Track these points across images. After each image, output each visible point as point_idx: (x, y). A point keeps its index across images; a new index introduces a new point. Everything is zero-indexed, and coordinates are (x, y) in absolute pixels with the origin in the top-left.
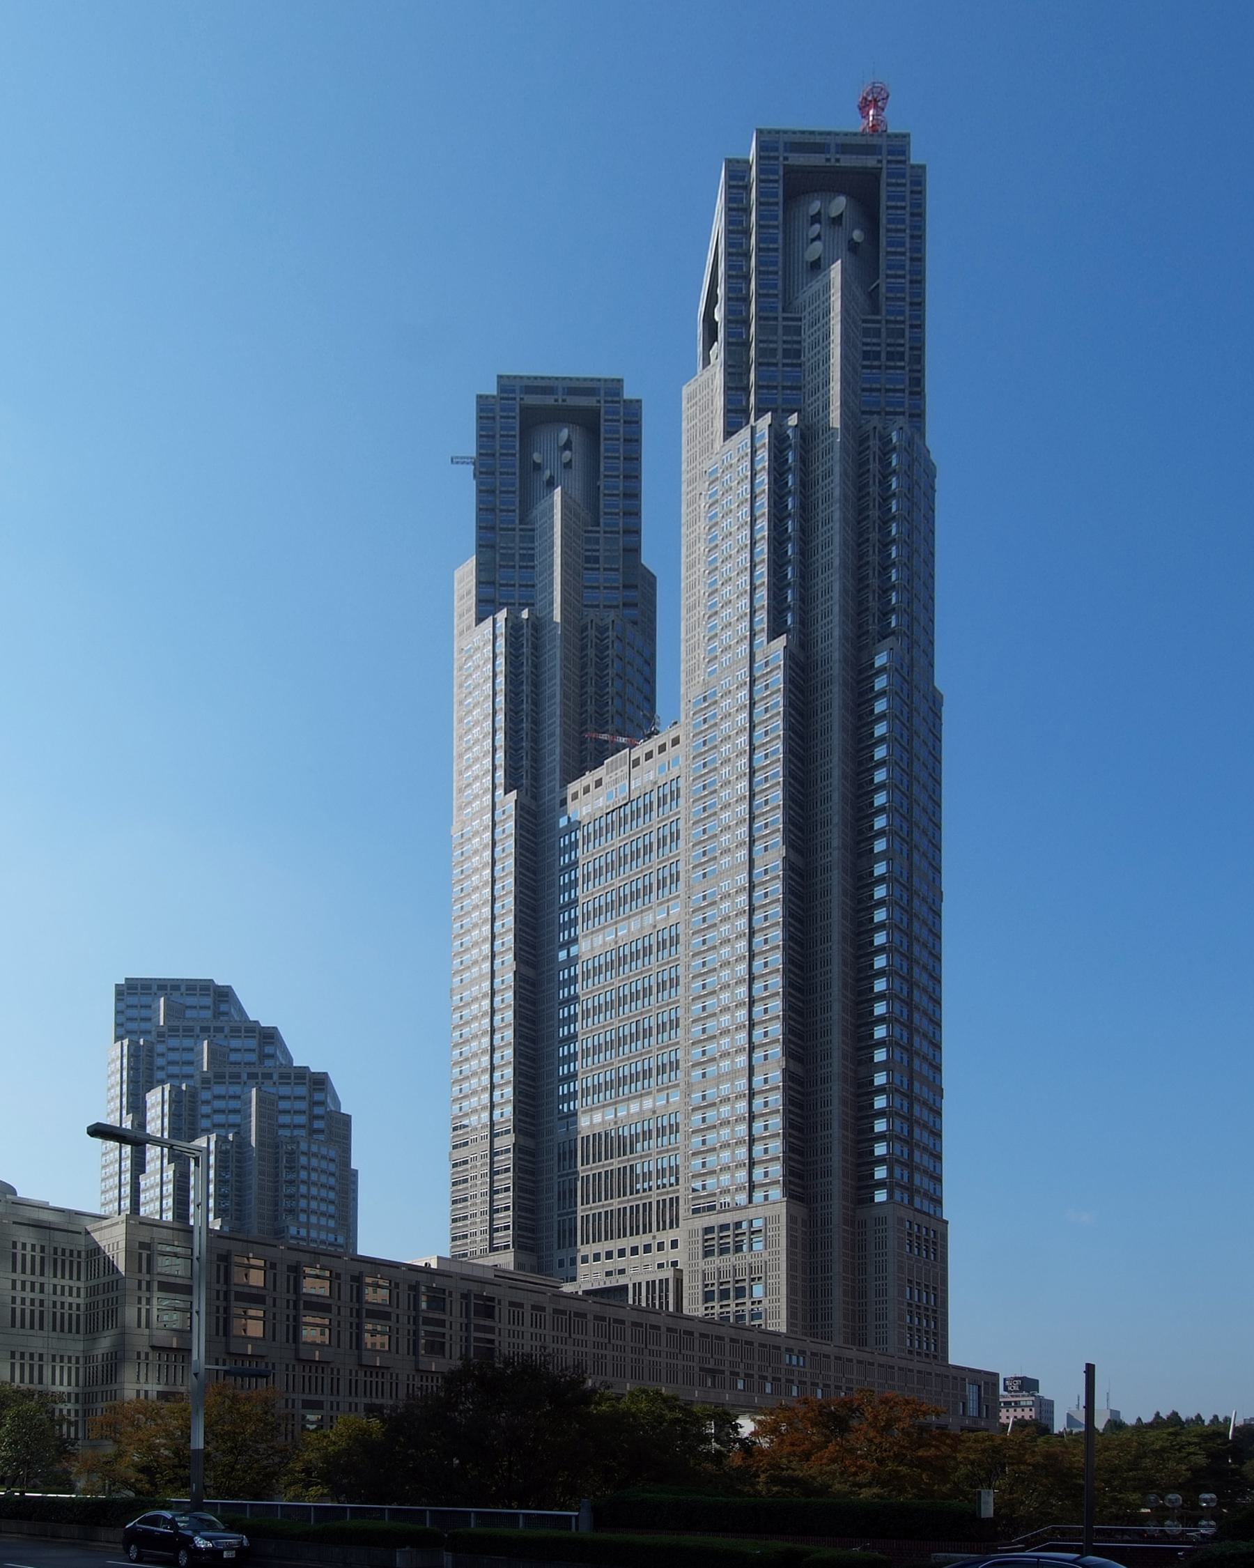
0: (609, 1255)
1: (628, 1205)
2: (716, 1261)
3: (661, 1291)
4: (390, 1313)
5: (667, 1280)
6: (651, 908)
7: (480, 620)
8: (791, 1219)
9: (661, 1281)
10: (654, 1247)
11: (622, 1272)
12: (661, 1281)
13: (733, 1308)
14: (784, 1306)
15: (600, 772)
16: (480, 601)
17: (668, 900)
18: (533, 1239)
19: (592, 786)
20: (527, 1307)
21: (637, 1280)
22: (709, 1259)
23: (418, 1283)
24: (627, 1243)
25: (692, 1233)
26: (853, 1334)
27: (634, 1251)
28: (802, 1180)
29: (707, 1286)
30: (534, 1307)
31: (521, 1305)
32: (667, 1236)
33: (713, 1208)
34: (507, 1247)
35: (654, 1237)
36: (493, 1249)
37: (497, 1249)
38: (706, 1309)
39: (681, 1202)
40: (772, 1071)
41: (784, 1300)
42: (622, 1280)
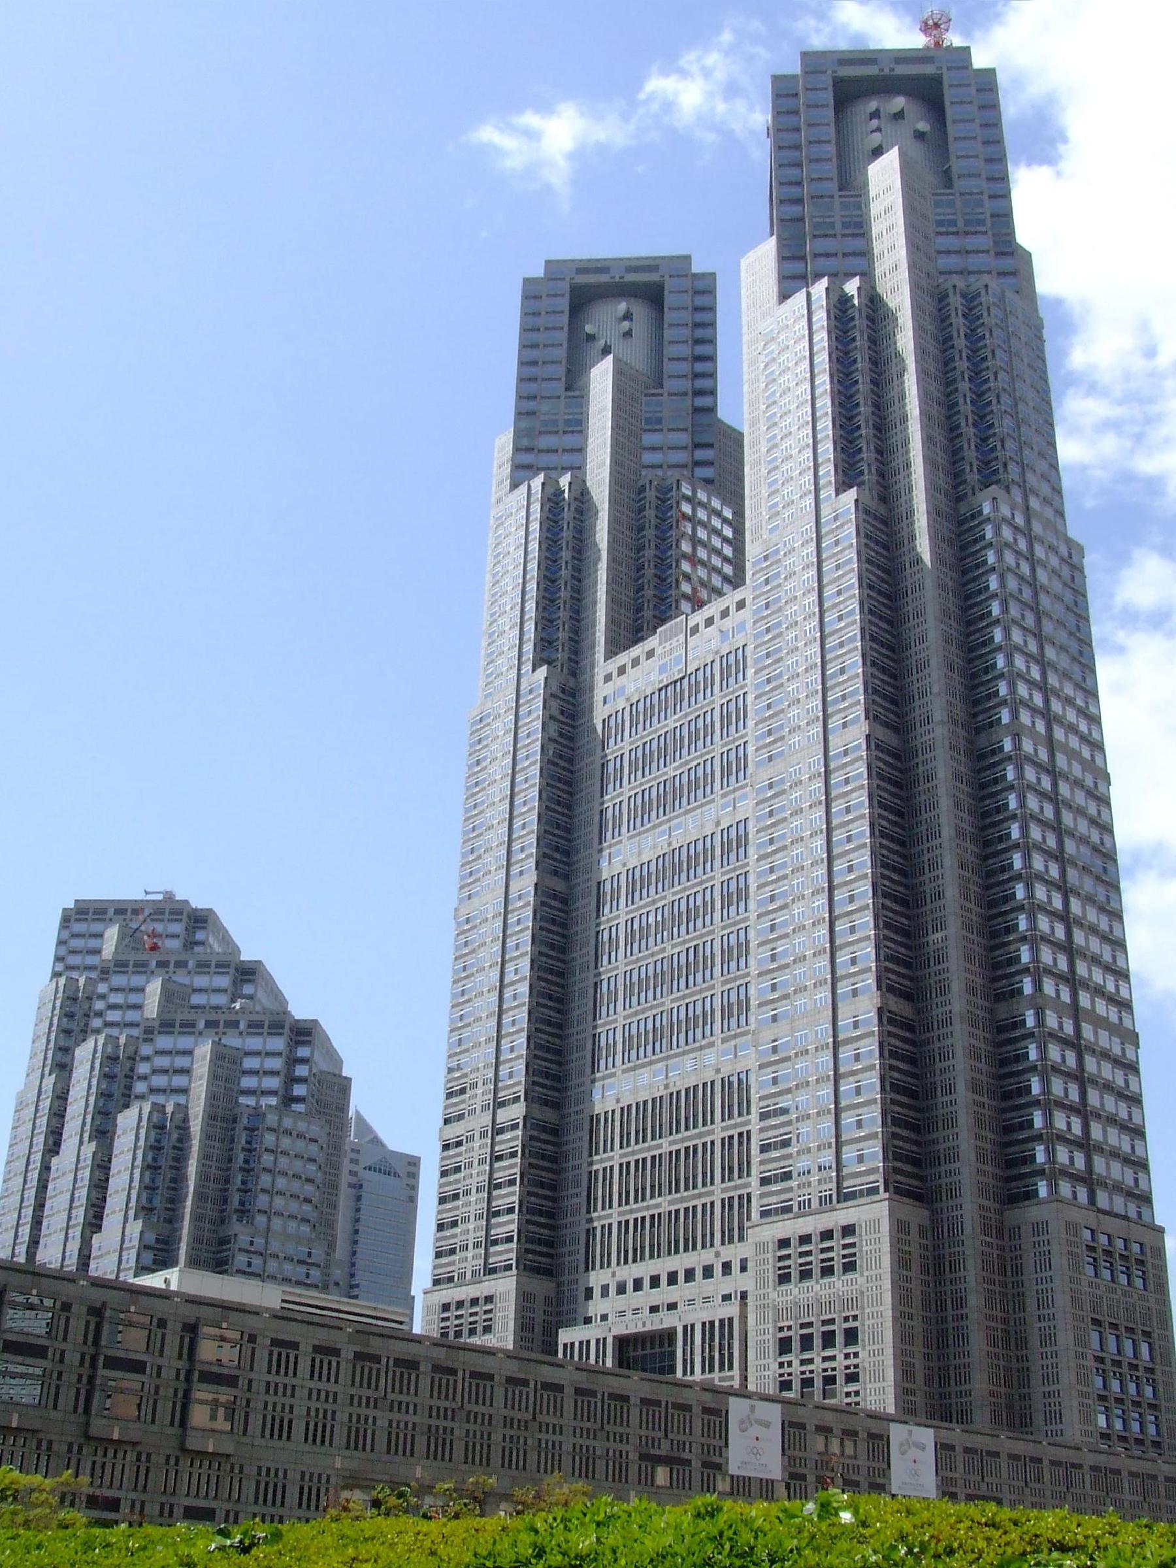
0: (655, 1282)
1: (681, 1207)
2: (795, 1291)
3: (722, 1336)
4: (144, 1364)
5: (731, 1320)
6: (713, 801)
7: (514, 486)
8: (900, 1228)
9: (722, 1321)
10: (718, 1270)
11: (672, 1306)
12: (722, 1321)
13: (818, 1365)
14: (890, 1361)
15: (652, 642)
16: (517, 467)
17: (734, 791)
18: (550, 1256)
19: (643, 658)
20: (305, 1348)
21: (689, 1319)
22: (783, 1288)
23: (104, 1304)
24: (679, 1262)
25: (761, 1247)
26: (1010, 1407)
27: (690, 1275)
28: (914, 1166)
29: (781, 1329)
30: (317, 1349)
31: (295, 1345)
32: (733, 1253)
33: (789, 1209)
34: (508, 1268)
35: (717, 1254)
36: (491, 1271)
37: (493, 1271)
38: (781, 1365)
39: (754, 1200)
40: (864, 1006)
41: (889, 1351)
42: (666, 1320)
